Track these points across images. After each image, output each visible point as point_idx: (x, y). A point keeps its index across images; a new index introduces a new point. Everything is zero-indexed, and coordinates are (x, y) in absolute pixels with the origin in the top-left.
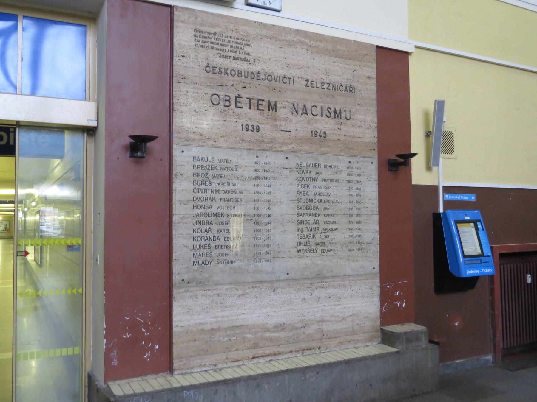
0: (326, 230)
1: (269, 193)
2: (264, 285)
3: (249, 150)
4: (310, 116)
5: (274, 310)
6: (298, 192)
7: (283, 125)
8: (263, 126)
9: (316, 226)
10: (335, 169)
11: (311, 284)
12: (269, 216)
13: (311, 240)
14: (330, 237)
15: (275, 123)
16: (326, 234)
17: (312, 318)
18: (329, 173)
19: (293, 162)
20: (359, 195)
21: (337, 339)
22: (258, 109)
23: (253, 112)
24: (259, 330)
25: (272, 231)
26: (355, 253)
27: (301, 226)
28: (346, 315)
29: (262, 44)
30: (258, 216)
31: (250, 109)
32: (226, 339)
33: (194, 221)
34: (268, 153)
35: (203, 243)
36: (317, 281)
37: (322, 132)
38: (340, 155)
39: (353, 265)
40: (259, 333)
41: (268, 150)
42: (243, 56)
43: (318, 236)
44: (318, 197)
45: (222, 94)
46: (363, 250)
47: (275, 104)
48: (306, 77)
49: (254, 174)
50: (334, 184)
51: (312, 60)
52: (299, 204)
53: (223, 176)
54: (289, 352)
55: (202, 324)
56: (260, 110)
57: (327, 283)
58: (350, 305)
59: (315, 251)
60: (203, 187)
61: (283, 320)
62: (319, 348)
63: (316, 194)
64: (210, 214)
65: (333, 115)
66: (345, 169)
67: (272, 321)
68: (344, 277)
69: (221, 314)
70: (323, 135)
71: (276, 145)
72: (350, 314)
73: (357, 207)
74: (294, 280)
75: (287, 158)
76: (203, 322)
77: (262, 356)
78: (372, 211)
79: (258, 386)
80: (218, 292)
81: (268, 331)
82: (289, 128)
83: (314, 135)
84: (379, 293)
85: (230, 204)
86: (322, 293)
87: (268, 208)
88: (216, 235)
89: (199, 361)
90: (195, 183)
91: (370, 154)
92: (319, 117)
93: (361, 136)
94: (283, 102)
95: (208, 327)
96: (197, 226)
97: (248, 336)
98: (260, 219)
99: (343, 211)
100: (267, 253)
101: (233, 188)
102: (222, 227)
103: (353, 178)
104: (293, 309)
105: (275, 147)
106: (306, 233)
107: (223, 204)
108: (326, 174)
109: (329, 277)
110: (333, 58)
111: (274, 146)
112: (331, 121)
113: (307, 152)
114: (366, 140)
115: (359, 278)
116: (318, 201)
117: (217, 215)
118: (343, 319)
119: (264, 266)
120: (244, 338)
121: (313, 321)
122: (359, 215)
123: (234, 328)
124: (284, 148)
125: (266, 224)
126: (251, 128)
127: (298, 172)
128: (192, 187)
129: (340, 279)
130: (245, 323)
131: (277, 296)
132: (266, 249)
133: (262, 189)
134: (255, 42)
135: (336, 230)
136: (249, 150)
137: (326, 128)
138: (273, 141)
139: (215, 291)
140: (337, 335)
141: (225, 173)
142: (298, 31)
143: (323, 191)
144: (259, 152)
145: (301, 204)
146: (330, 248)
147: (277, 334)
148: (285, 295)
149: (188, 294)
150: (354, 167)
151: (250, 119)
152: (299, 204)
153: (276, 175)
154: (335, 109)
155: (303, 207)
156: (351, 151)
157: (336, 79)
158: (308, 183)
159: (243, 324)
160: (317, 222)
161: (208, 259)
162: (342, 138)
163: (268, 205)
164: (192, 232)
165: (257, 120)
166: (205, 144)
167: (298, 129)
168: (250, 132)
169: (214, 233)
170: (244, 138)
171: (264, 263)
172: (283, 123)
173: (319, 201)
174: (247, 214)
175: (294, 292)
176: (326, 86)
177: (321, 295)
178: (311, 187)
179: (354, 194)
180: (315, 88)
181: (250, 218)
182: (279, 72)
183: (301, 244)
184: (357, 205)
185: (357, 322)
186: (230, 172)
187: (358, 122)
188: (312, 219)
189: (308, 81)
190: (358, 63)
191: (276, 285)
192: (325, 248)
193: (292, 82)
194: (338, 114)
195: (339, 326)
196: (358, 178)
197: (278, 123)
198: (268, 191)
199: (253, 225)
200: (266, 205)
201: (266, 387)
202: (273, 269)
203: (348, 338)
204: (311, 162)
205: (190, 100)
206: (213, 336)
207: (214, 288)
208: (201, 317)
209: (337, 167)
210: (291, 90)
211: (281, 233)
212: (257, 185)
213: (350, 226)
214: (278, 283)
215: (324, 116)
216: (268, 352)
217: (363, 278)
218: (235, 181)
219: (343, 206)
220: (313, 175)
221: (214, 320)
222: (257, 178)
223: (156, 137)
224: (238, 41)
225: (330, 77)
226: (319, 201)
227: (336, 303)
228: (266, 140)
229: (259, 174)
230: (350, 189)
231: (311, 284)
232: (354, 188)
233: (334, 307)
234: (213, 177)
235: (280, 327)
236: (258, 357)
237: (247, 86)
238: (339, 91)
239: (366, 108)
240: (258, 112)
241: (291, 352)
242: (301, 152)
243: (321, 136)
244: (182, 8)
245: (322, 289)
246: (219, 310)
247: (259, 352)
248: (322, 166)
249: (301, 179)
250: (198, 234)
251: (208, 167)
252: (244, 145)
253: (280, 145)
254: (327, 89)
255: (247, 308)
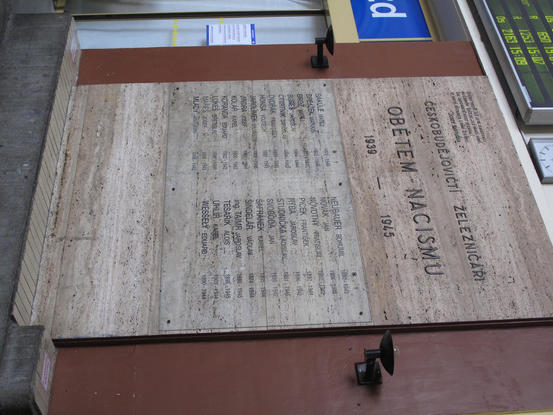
0: (237, 240)
1: (287, 165)
2: (162, 164)
3: (342, 143)
4: (412, 213)
5: (125, 176)
6: (293, 200)
7: (387, 179)
8: (378, 157)
9: (244, 224)
10: (337, 251)
11: (154, 222)
12: (256, 166)
13: (223, 218)
14: (227, 247)
15: (386, 170)
16: (231, 240)
17: (103, 224)
18: (330, 242)
19: (335, 193)
20: (300, 291)
21: (59, 261)
22: (398, 153)
23: (392, 148)
24: (102, 159)
25: (235, 171)
26: (199, 288)
27: (243, 206)
28: (95, 276)
29: (487, 154)
30: (256, 154)
31: (396, 143)
32: (99, 128)
33: (246, 96)
34: (342, 164)
35: (220, 104)
36: (158, 229)
37: (393, 231)
38: (362, 258)
39: (178, 285)
40: (97, 161)
41: (346, 162)
42: (461, 134)
43: (228, 228)
44: (288, 226)
45: (404, 116)
46: (203, 301)
47: (412, 170)
48: (468, 205)
49: (310, 149)
50: (313, 249)
51: (497, 214)
52: (275, 201)
53: (303, 119)
54: (60, 195)
55: (124, 106)
56: (398, 154)
57: (152, 244)
58: (110, 282)
59: (205, 225)
60: (287, 103)
61: (108, 187)
62: (53, 235)
63: (293, 224)
64: (255, 109)
65: (425, 246)
66: (341, 266)
67: (110, 175)
68: (160, 270)
69: (132, 122)
70: (388, 231)
71: (355, 172)
72: (96, 282)
73: (279, 289)
74: (164, 199)
75: (340, 184)
76: (126, 107)
77: (65, 164)
78: (274, 317)
79: (37, 112)
80: (159, 119)
81: (98, 170)
82: (385, 187)
83: (385, 219)
84: (121, 334)
85: (269, 127)
86: (138, 238)
87: (267, 165)
88: (229, 115)
89: (80, 105)
90: (290, 96)
91: (377, 311)
92: (414, 226)
93: (404, 294)
94: (420, 179)
95: (119, 111)
96: (240, 99)
97: (97, 149)
98: (251, 157)
99: (269, 265)
100: (205, 166)
101: (289, 128)
102: (239, 120)
103: (328, 281)
104: (121, 198)
105: (353, 172)
106: (232, 212)
107: (268, 120)
108: (327, 238)
109: (162, 246)
110: (516, 244)
111: (354, 170)
112: (414, 244)
113: (355, 210)
114: (399, 303)
115: (154, 298)
116: (283, 226)
117: (254, 115)
118: (89, 271)
119: (188, 163)
120: (96, 145)
121: (98, 225)
122: (264, 293)
123: (112, 134)
124: (353, 182)
125: (245, 164)
126: (371, 145)
127: (323, 200)
128: (286, 94)
129: (156, 263)
130: (114, 146)
131: (144, 179)
132: (210, 164)
133: (291, 158)
134: (486, 146)
135: (239, 255)
136: (342, 143)
137: (400, 236)
138: (361, 169)
139: (161, 116)
140: (64, 262)
141: (307, 121)
142: (531, 194)
143: (300, 234)
144: (342, 153)
145: (276, 204)
146: (209, 245)
147: (90, 180)
148: (143, 188)
149: (161, 95)
150: (348, 282)
151: (382, 144)
152: (275, 201)
153: (314, 173)
154: (436, 249)
155: (272, 206)
156: (373, 277)
157: (485, 249)
158: (308, 212)
159: (114, 143)
160: (250, 226)
161: (201, 109)
162: (391, 261)
163: (270, 165)
164: (232, 94)
165: (383, 151)
166: (338, 103)
167: (387, 198)
168: (366, 144)
169: (231, 113)
170: (355, 138)
171: (191, 162)
172: (389, 180)
173: (284, 229)
174: (257, 143)
175: (146, 199)
176: (467, 234)
177: (135, 236)
178: (304, 217)
179: (301, 284)
180: (457, 220)
181: (252, 146)
182: (460, 174)
183: (217, 205)
184: (281, 289)
185: (79, 295)
186: (308, 126)
187: (427, 287)
188: (255, 219)
189: (463, 210)
190: (530, 286)
191: (160, 177)
192: (208, 239)
193: (453, 189)
194: (429, 253)
195: (79, 265)
196: (329, 289)
197: (387, 174)
198: (290, 164)
199: (243, 150)
200: (271, 163)
201: (32, 120)
202: (183, 172)
203: (55, 281)
204: (342, 216)
205: (386, 90)
206: (106, 116)
207: (165, 115)
208: (133, 105)
209: (342, 253)
210: (441, 188)
211: (233, 181)
212: (296, 153)
213: (245, 278)
214: (161, 181)
215: (419, 233)
216: (69, 170)
217: (153, 304)
218: (298, 130)
219: (278, 265)
220: (322, 220)
221: (126, 116)
222: (306, 152)
223: (332, 54)
224: (478, 130)
225: (483, 240)
226: (284, 229)
227: (118, 258)
228: (360, 161)
229: (311, 155)
230: (309, 276)
231: (154, 222)
232: (312, 283)
233: (113, 255)
234: (300, 111)
235: (99, 183)
236: (66, 159)
237: (425, 140)
238: (468, 255)
239: (456, 300)
240: (395, 152)
241: (60, 198)
242: (353, 202)
243: (385, 228)
244: (488, 81)
245: (144, 237)
246: (137, 120)
247: (72, 161)
248: (338, 232)
249: (313, 204)
250: (230, 100)
251: (312, 106)
252: (347, 140)
253: (357, 177)
254: (464, 237)
255: (134, 147)
